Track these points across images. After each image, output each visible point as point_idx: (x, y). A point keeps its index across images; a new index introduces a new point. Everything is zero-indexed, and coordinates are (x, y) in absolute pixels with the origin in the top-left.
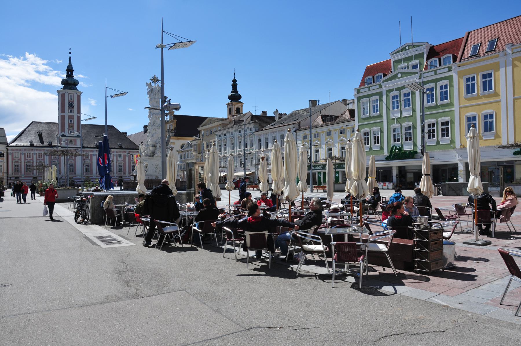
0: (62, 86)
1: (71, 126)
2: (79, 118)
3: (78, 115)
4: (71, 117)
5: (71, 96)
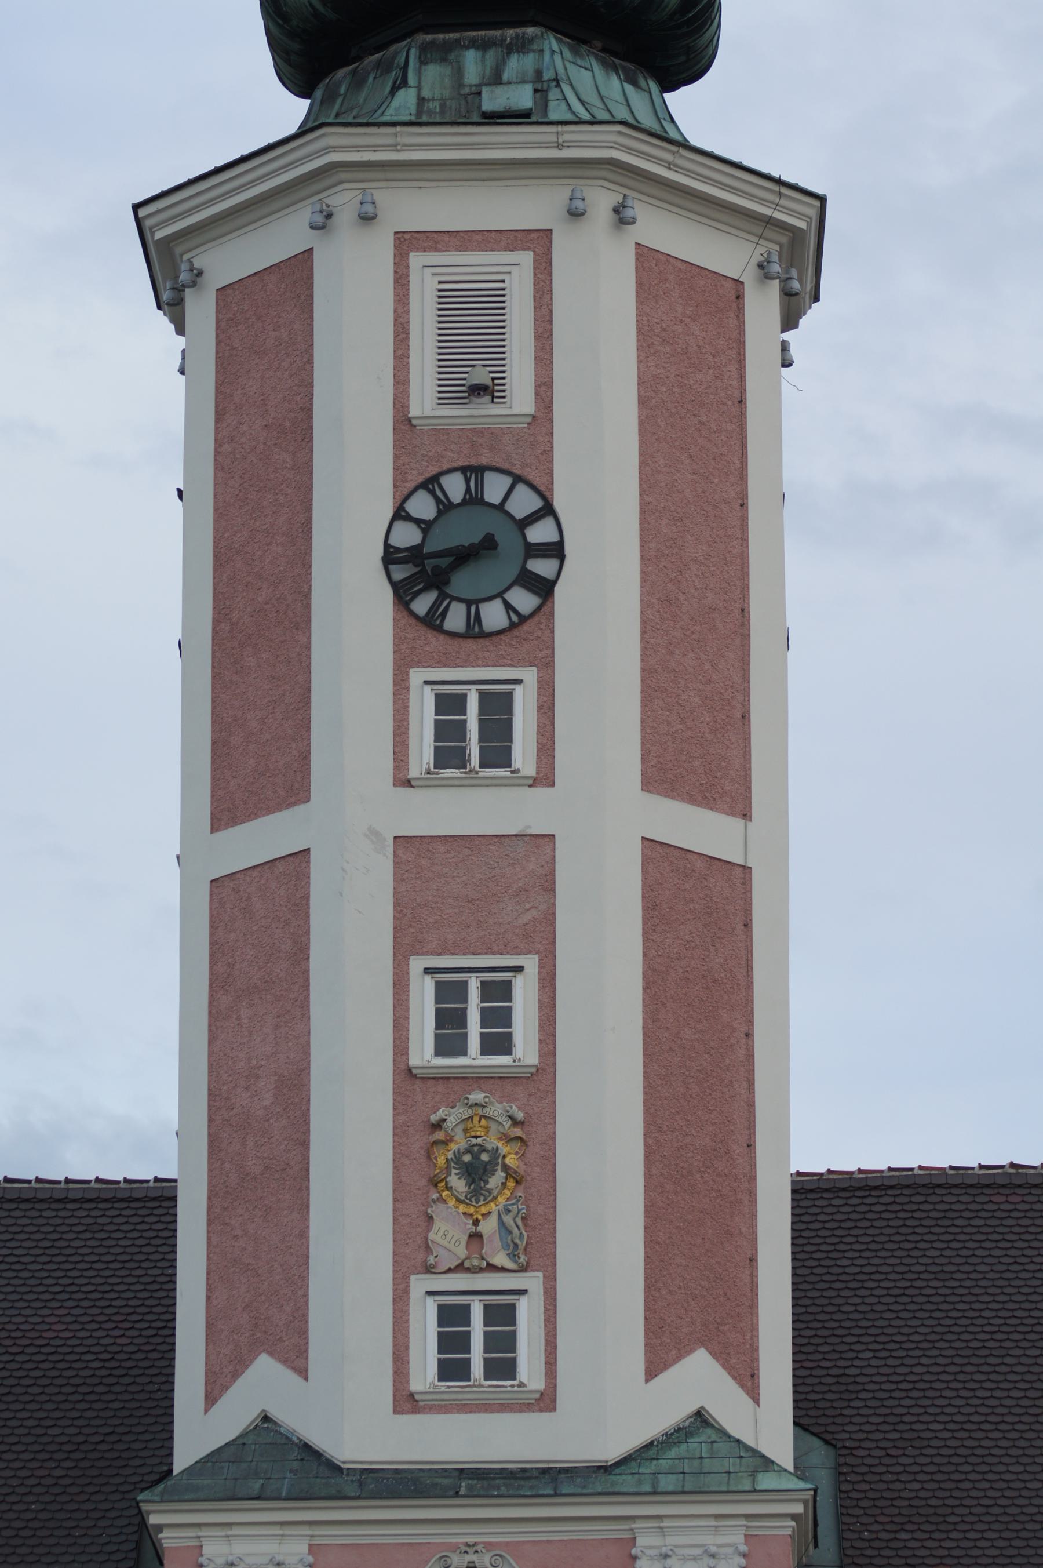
0: (291, 111)
1: (474, 1160)
2: (705, 942)
3: (699, 829)
4: (474, 909)
5: (471, 315)
